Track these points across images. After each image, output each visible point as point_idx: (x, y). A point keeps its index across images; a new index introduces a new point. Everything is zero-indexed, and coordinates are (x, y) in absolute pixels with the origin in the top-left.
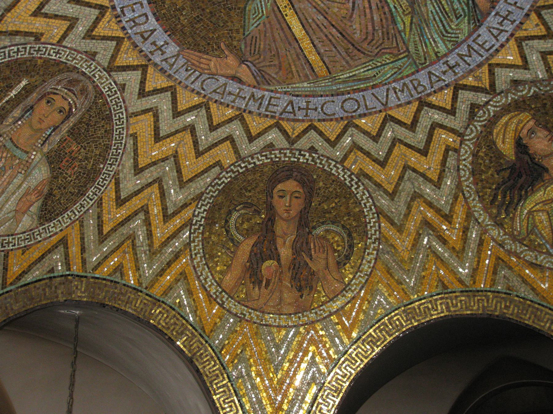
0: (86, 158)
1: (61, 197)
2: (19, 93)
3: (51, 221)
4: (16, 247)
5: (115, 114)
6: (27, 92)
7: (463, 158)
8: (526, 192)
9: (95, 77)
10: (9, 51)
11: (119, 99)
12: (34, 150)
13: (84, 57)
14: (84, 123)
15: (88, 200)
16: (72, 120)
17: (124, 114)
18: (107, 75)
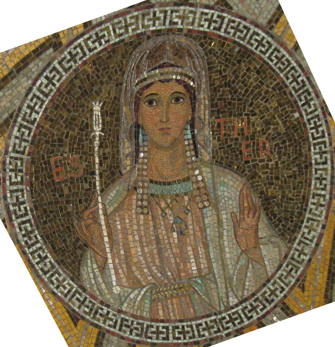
0: (268, 123)
1: (284, 192)
2: (103, 124)
3: (300, 227)
4: (287, 289)
5: (249, 42)
6: (112, 114)
9: (177, 23)
10: (39, 89)
11: (234, 22)
12: (194, 169)
13: (136, 14)
14: (221, 86)
15: (321, 167)
16: (202, 96)
17: (260, 32)
18: (188, 8)
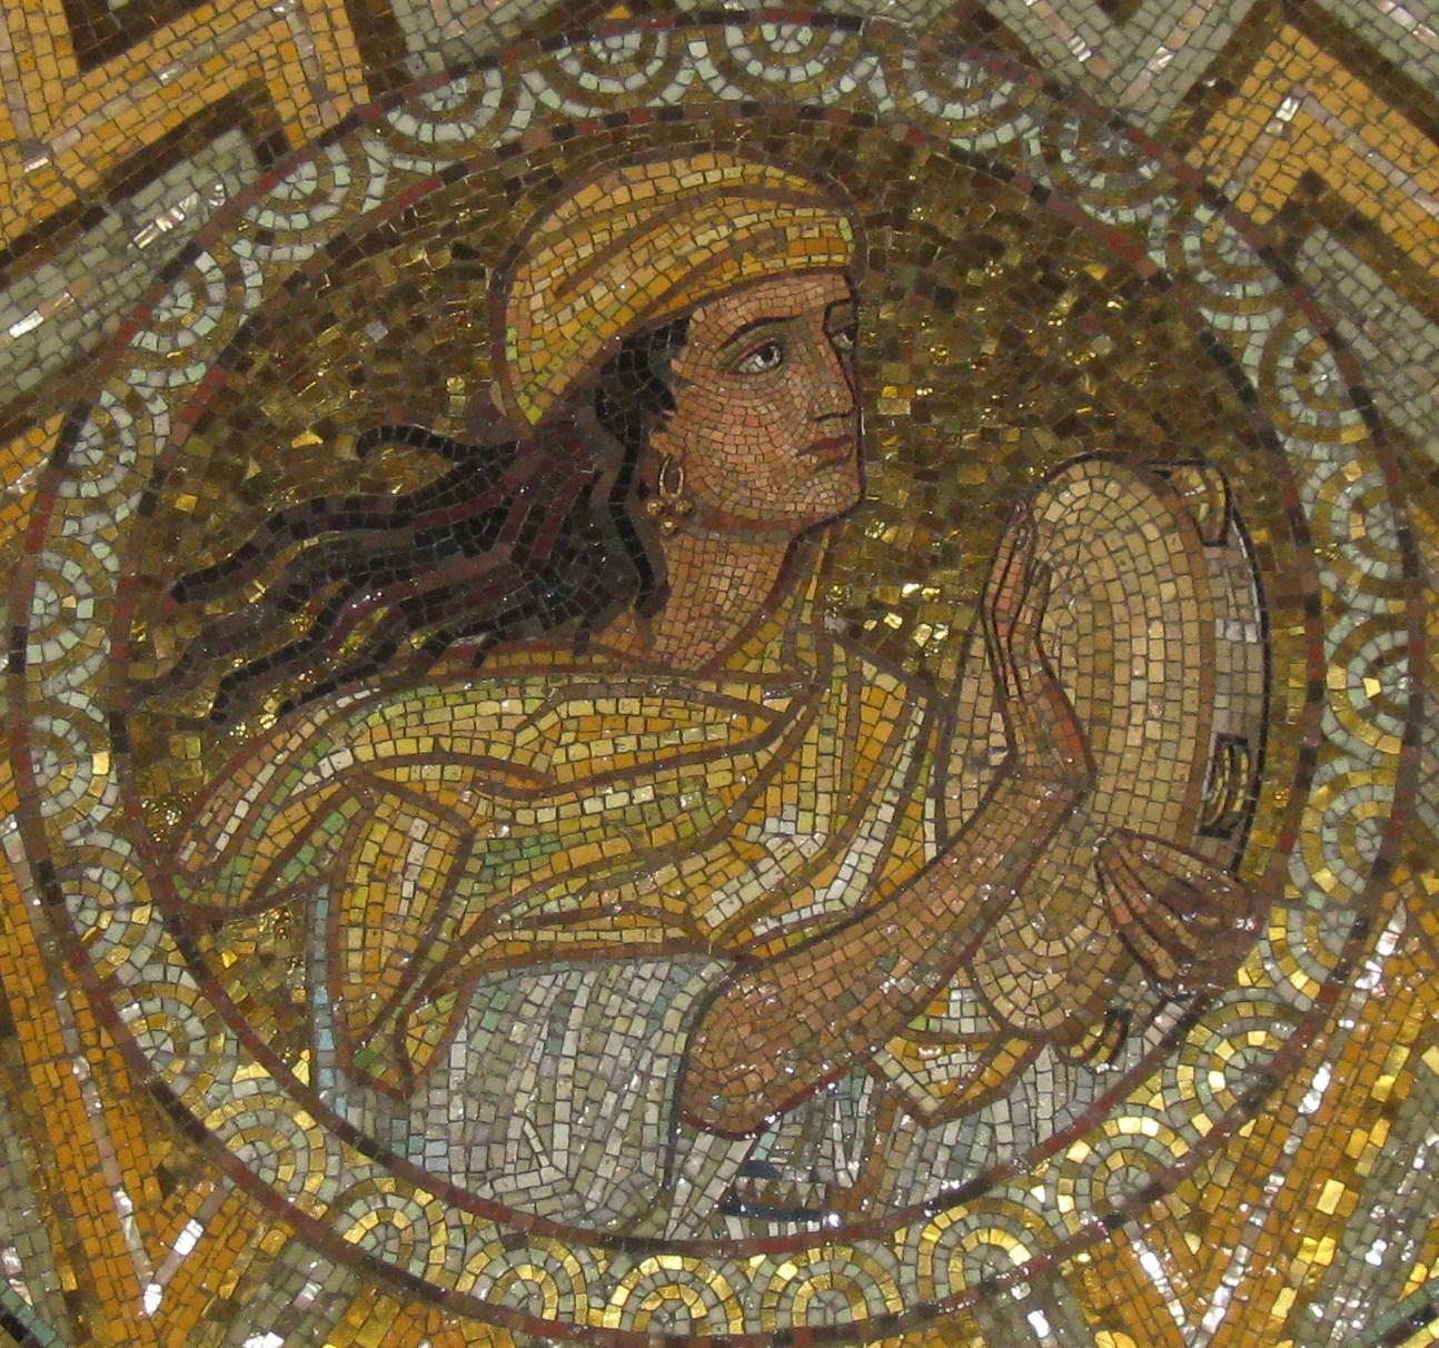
7: (268, 220)
8: (435, 650)
